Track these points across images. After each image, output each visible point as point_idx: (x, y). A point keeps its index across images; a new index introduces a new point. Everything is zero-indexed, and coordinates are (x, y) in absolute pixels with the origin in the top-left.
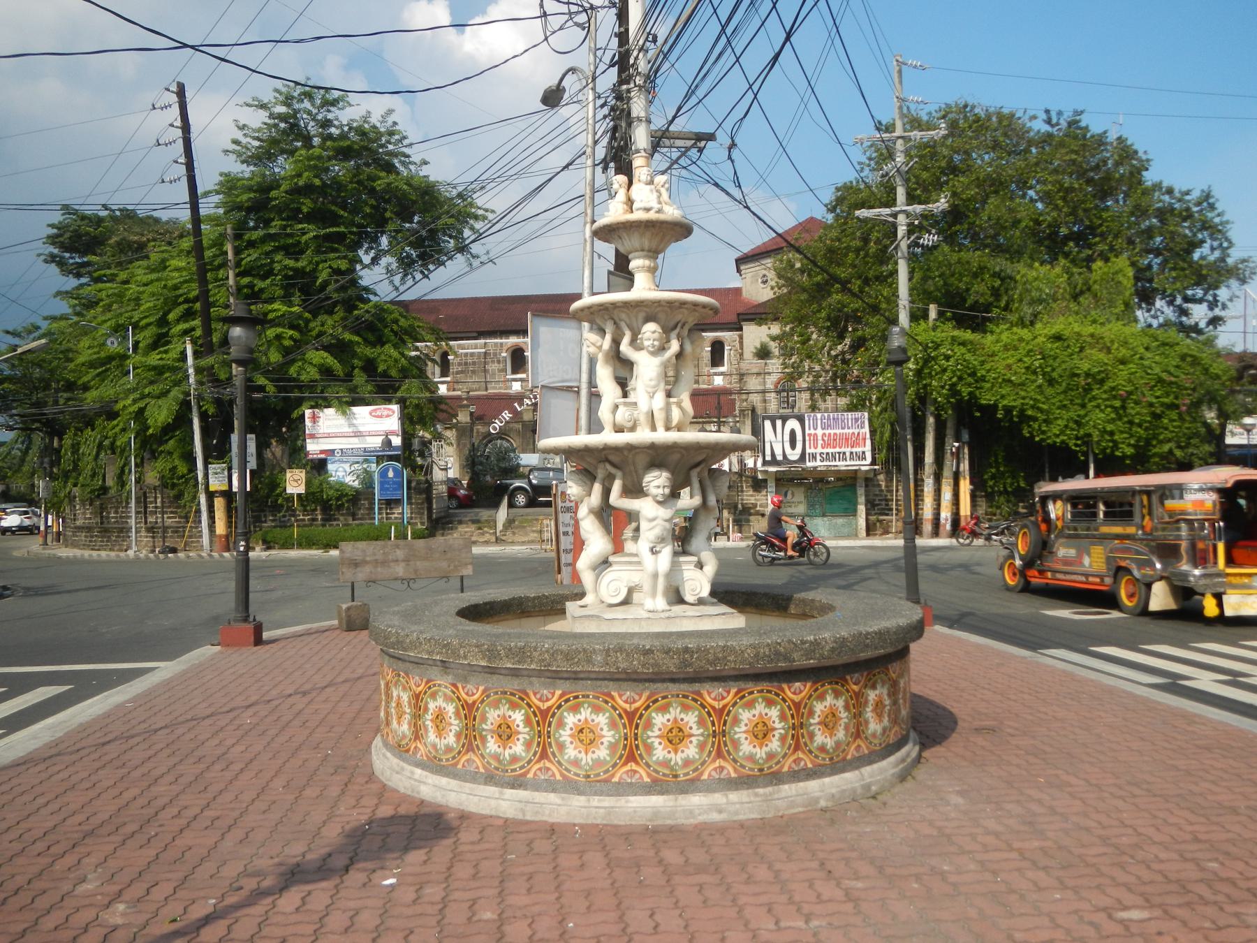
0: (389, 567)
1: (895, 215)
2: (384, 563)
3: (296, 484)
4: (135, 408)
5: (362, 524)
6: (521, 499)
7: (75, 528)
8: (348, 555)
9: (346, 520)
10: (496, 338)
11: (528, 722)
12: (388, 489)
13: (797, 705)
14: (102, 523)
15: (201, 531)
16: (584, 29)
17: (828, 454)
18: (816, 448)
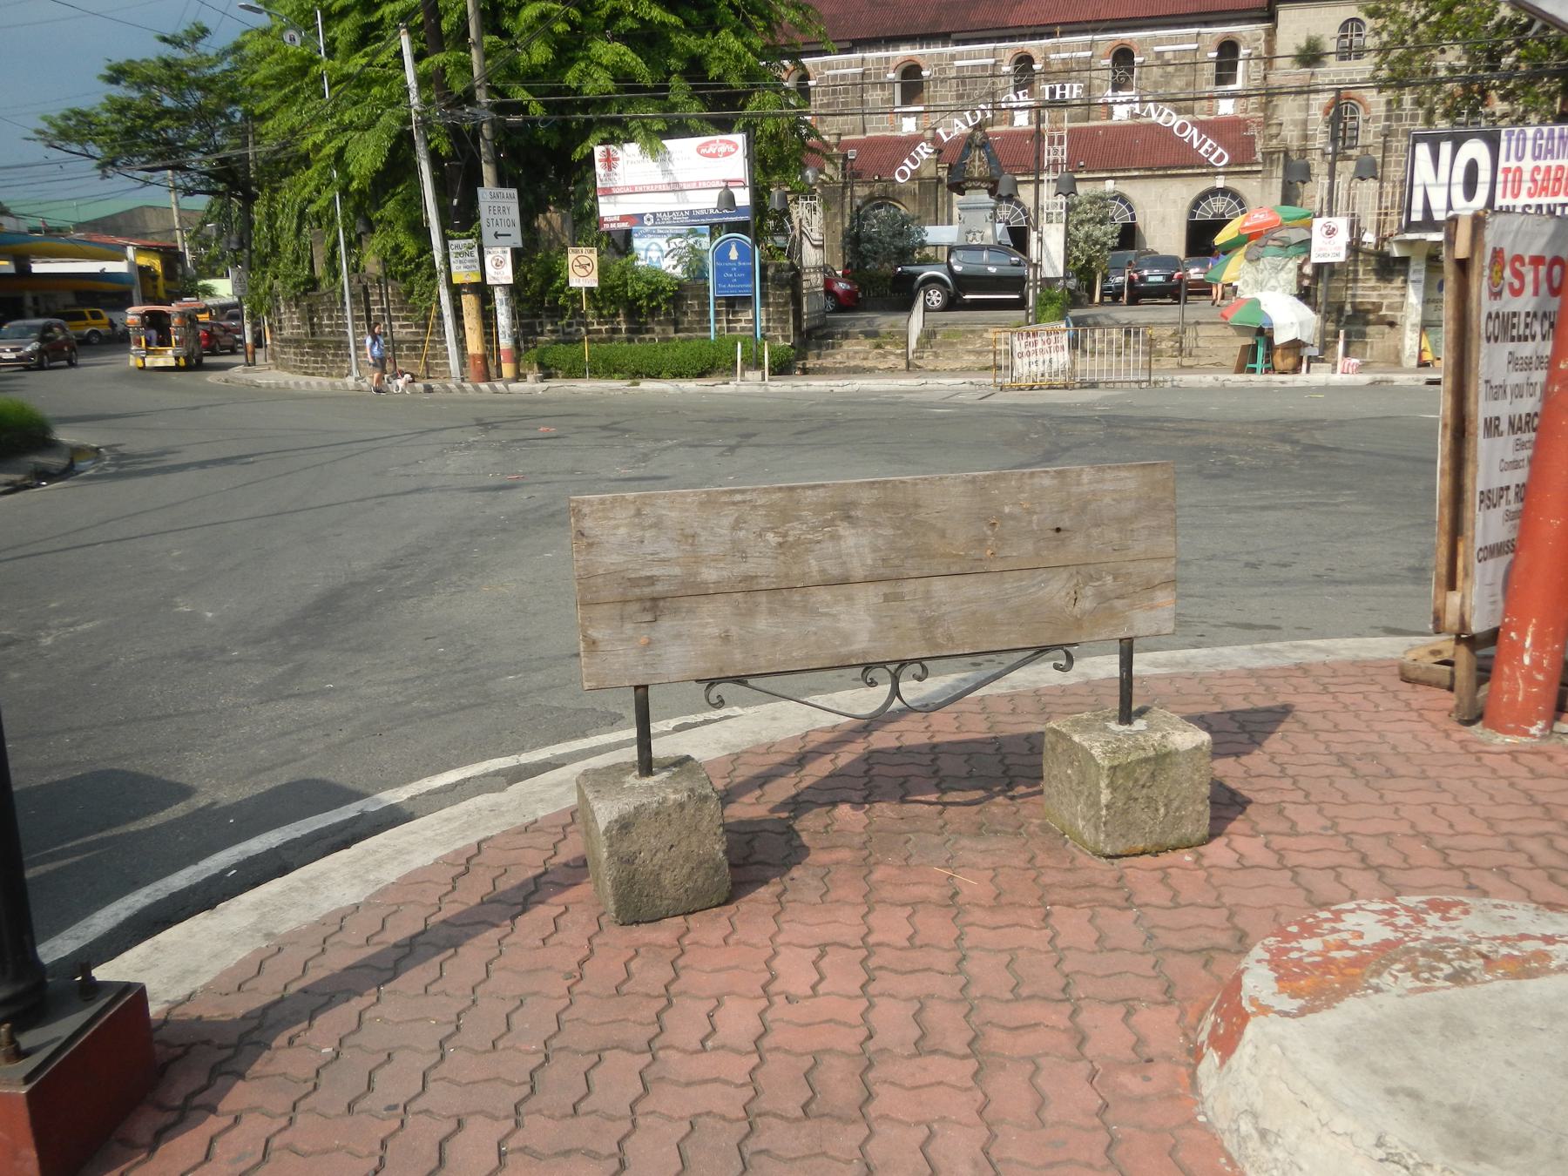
0: (809, 611)
2: (784, 591)
3: (582, 272)
4: (329, 149)
5: (689, 339)
6: (936, 297)
7: (282, 341)
8: (610, 559)
9: (663, 330)
10: (879, 49)
12: (729, 280)
14: (313, 334)
15: (446, 349)
17: (1540, 207)
18: (1516, 196)
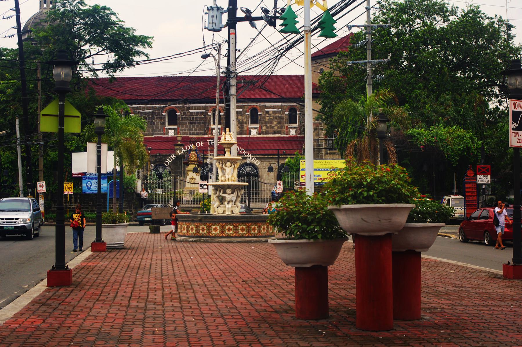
1: (365, 64)
3: (68, 190)
11: (207, 228)
13: (249, 226)
16: (217, 51)
